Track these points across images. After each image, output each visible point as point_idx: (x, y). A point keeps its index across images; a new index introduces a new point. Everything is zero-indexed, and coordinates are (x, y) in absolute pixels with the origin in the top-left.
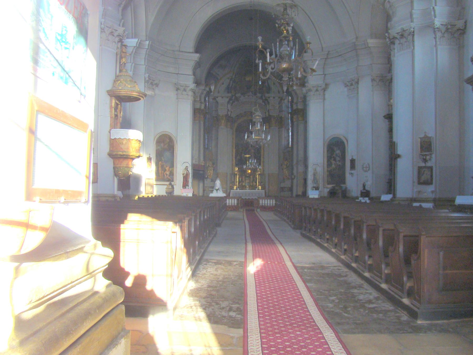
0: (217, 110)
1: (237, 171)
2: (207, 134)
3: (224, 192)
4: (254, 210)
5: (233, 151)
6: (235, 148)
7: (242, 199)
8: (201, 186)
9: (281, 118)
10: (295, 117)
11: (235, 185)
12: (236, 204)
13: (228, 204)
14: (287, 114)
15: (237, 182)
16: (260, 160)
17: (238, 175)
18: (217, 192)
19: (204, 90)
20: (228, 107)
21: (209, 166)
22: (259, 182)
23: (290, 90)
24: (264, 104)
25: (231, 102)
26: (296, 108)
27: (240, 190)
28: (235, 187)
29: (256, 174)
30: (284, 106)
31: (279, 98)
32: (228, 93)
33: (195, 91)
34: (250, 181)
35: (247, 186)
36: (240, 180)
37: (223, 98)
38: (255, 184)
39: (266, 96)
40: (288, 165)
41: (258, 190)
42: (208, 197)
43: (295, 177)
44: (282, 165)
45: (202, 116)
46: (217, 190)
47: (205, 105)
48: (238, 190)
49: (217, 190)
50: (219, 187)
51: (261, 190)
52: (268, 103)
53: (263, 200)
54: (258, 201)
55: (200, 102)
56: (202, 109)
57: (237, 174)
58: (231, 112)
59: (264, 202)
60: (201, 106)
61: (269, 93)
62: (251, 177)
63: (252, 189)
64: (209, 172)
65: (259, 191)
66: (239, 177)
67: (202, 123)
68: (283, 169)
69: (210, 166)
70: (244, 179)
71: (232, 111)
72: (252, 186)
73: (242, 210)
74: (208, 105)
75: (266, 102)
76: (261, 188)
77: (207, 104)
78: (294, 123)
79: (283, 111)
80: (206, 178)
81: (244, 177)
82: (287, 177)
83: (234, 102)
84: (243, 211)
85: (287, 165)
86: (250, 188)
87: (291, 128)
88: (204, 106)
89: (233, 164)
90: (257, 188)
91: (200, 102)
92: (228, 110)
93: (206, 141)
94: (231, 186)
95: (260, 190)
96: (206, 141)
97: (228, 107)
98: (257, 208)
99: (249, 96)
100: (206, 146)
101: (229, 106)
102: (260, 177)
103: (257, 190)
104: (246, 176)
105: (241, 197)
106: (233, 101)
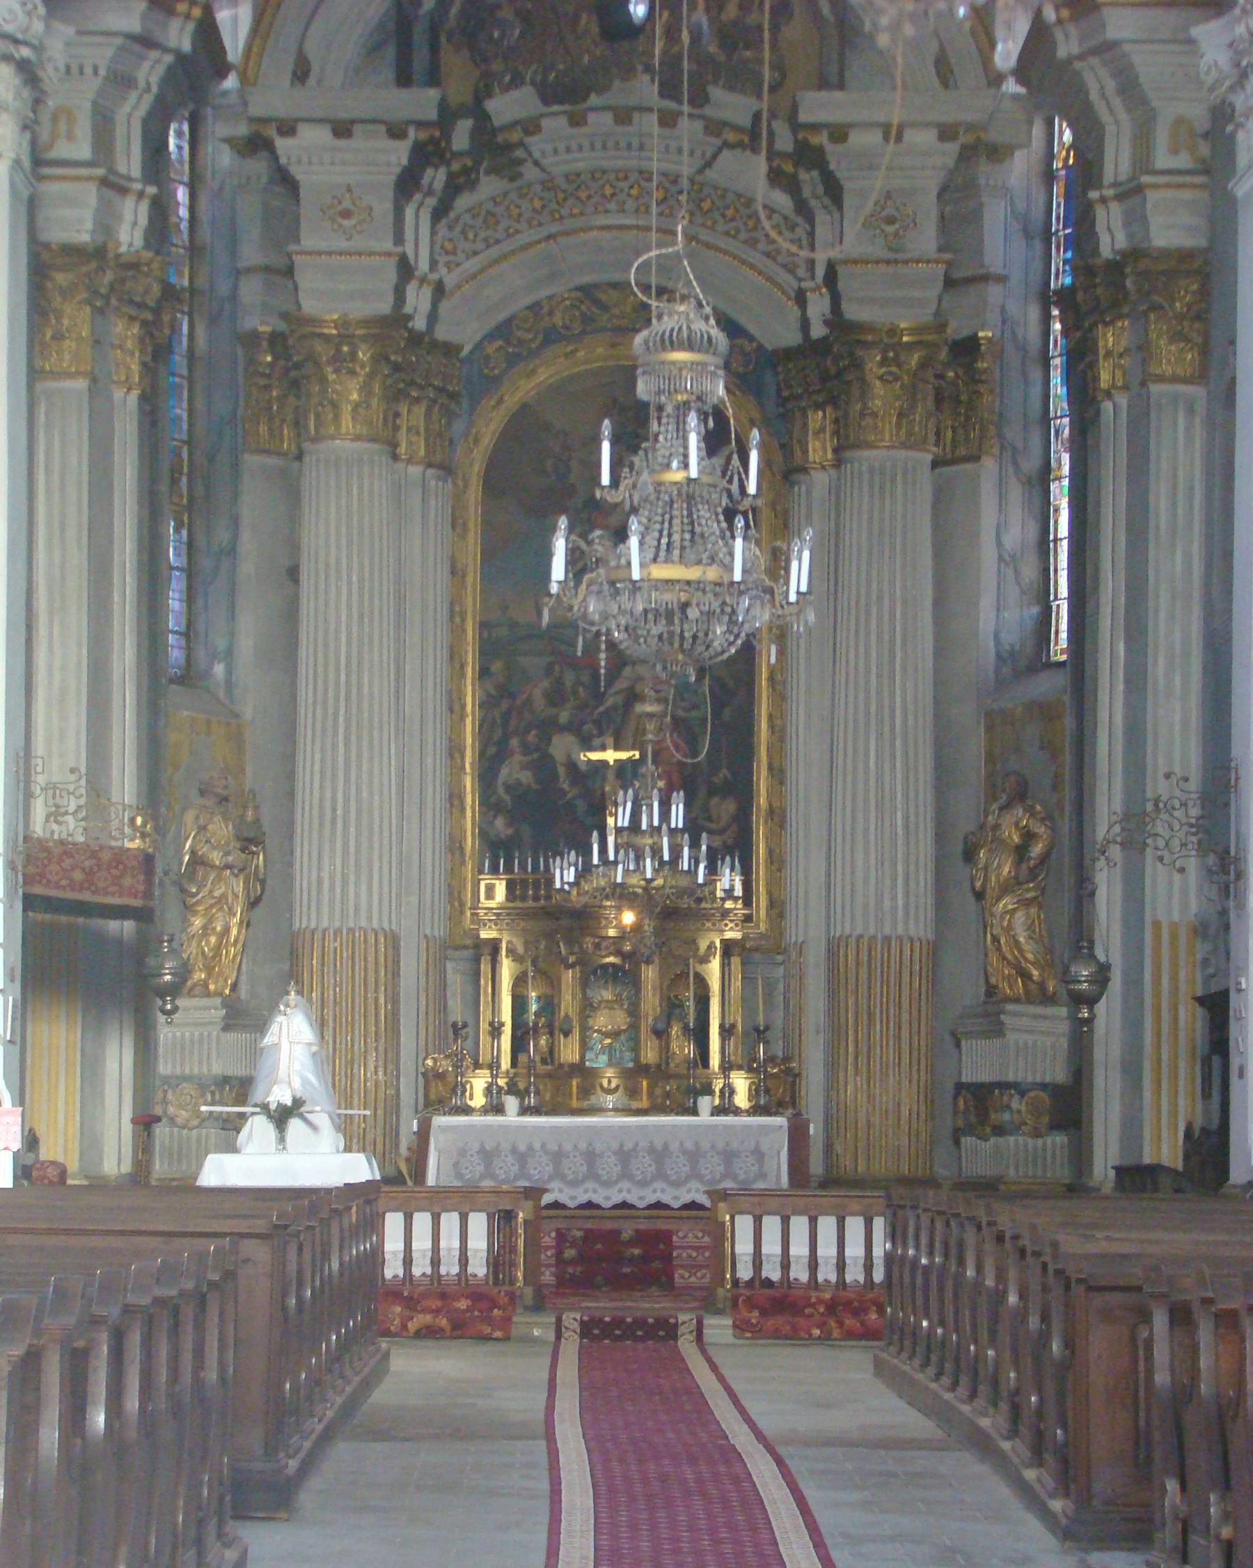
0: (289, 272)
1: (499, 916)
2: (177, 530)
3: (353, 1138)
4: (666, 1330)
5: (454, 707)
6: (484, 672)
7: (556, 1205)
8: (111, 1065)
9: (967, 348)
10: (1109, 339)
11: (477, 1065)
12: (478, 1268)
13: (393, 1269)
14: (1034, 313)
15: (496, 1031)
16: (742, 791)
17: (511, 952)
18: (282, 1140)
19: (146, 42)
20: (409, 234)
21: (198, 861)
22: (726, 1031)
23: (1067, 46)
24: (782, 200)
25: (436, 177)
26: (1121, 242)
27: (524, 1111)
28: (479, 1083)
29: (703, 945)
30: (995, 217)
31: (946, 133)
32: (404, 79)
33: (39, 48)
34: (634, 1012)
35: (610, 1076)
36: (534, 1007)
37: (342, 130)
38: (690, 1050)
39: (804, 117)
40: (1037, 849)
41: (717, 1111)
42: (188, 1188)
43: (1102, 976)
44: (969, 855)
45: (124, 332)
46: (281, 1117)
47: (161, 209)
48: (511, 1115)
49: (281, 1117)
50: (305, 1081)
51: (756, 1110)
52: (834, 191)
53: (772, 1225)
54: (720, 1236)
55: (104, 182)
56: (123, 249)
57: (494, 946)
58: (439, 291)
59: (771, 1247)
60: (106, 223)
61: (841, 86)
62: (650, 974)
63: (656, 1108)
64: (207, 929)
65: (729, 1119)
66: (519, 982)
67: (127, 403)
68: (979, 896)
69: (216, 857)
70: (568, 1003)
71: (450, 280)
72: (659, 1073)
73: (541, 1328)
74: (184, 212)
75: (809, 179)
76: (754, 1093)
77: (182, 194)
78: (1107, 406)
79: (985, 278)
80: (163, 992)
81: (569, 976)
82: (1026, 976)
83: (454, 187)
84: (551, 1336)
85: (1021, 852)
86: (633, 1092)
87: (1066, 458)
88: (143, 221)
89: (455, 846)
90: (709, 1091)
91: (100, 172)
92: (405, 270)
93: (175, 602)
94: (432, 1077)
95: (737, 1111)
96: (175, 602)
97: (399, 239)
98: (708, 1303)
99: (623, 116)
100: (176, 655)
101: (417, 217)
102: (737, 983)
103: (705, 1117)
104: (592, 974)
105: (532, 1193)
106: (456, 166)
